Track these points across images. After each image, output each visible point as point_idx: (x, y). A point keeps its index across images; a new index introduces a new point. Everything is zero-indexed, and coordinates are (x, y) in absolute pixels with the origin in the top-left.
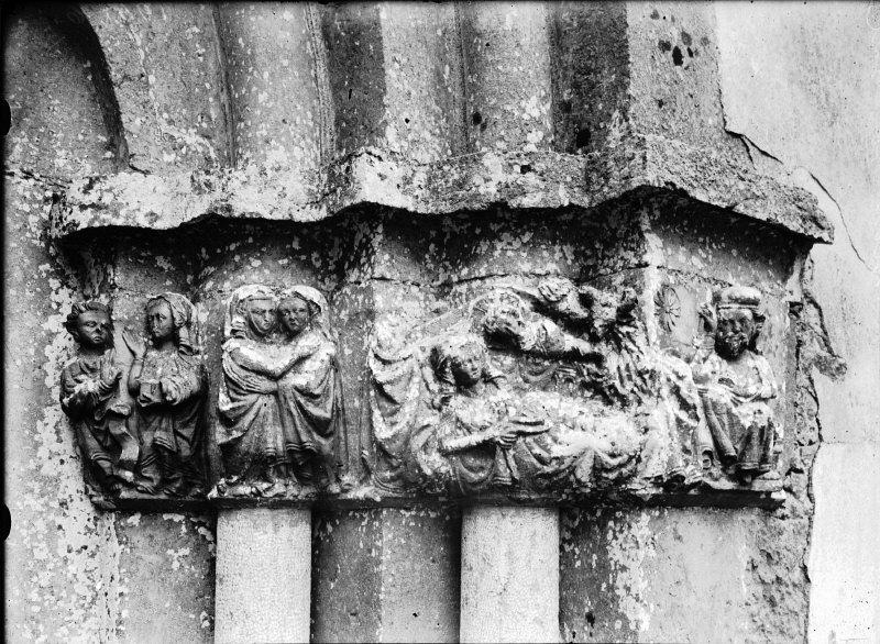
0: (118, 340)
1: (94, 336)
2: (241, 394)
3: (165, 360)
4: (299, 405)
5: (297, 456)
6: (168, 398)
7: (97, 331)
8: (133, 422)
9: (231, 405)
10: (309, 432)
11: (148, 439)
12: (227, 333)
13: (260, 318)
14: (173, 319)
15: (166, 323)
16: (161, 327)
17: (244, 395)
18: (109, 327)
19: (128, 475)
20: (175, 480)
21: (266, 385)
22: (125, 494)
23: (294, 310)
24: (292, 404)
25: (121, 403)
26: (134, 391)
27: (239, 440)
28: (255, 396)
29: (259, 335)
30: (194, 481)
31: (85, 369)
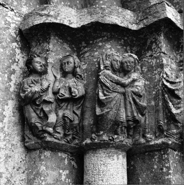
0: (49, 70)
1: (39, 68)
2: (109, 92)
3: (71, 82)
4: (134, 100)
5: (131, 123)
6: (73, 94)
7: (41, 66)
8: (53, 106)
9: (104, 98)
10: (137, 112)
11: (61, 113)
12: (102, 68)
13: (115, 63)
14: (75, 63)
15: (72, 65)
16: (68, 68)
17: (111, 93)
18: (46, 65)
19: (51, 130)
20: (69, 135)
21: (122, 90)
22: (49, 139)
23: (129, 62)
24: (131, 98)
25: (49, 97)
26: (55, 93)
27: (108, 113)
28: (117, 94)
29: (114, 71)
30: (76, 137)
31: (34, 82)
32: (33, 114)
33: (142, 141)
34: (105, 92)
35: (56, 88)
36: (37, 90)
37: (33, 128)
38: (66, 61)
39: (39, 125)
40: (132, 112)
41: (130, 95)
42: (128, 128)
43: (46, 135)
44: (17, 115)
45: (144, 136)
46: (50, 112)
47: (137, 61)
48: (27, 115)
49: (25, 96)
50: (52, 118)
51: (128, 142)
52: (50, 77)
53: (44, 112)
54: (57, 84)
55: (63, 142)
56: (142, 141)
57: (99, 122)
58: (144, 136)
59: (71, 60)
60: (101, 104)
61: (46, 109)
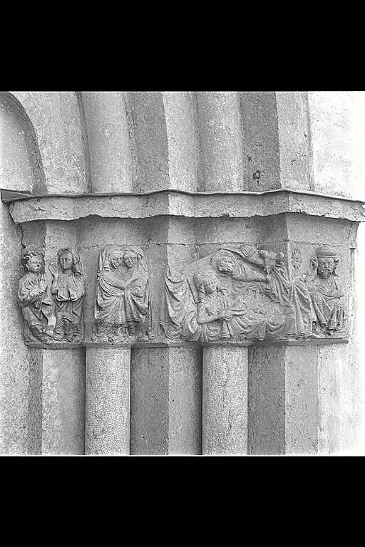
3: (71, 279)
4: (133, 301)
7: (38, 266)
12: (101, 269)
16: (67, 265)
19: (51, 332)
25: (48, 299)
32: (33, 317)
33: (146, 338)
34: (104, 297)
35: (54, 291)
36: (35, 293)
37: (33, 330)
38: (64, 257)
39: (39, 328)
40: (131, 313)
41: (129, 297)
42: (129, 328)
43: (47, 338)
44: (16, 314)
45: (147, 334)
46: (49, 314)
47: (139, 256)
48: (26, 317)
49: (24, 299)
50: (52, 321)
51: (131, 339)
52: (47, 276)
53: (44, 315)
54: (55, 284)
55: (65, 342)
56: (146, 338)
57: (98, 324)
58: (147, 334)
59: (69, 256)
60: (100, 308)
61: (45, 312)
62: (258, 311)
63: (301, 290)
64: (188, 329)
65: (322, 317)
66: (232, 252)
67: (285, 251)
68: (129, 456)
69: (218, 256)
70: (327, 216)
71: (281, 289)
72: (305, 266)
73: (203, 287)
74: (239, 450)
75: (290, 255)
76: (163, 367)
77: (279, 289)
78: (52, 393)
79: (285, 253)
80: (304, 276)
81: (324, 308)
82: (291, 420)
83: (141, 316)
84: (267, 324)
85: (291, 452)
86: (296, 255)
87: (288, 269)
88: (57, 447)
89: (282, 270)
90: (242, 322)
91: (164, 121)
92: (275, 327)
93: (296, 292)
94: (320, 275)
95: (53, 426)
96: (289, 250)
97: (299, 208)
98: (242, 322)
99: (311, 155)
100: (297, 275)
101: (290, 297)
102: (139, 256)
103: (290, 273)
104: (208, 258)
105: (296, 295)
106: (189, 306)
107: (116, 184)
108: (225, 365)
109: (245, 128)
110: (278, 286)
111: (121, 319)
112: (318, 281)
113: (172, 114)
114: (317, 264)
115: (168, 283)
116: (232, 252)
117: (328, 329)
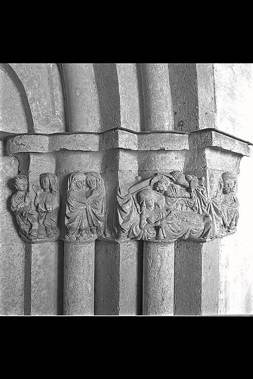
46: (33, 221)
47: (98, 179)
62: (185, 220)
63: (216, 204)
64: (133, 233)
65: (226, 221)
66: (167, 176)
67: (205, 176)
68: (93, 315)
69: (155, 180)
70: (232, 151)
71: (201, 203)
72: (216, 186)
73: (144, 203)
74: (168, 312)
75: (208, 178)
76: (116, 257)
77: (199, 203)
78: (39, 273)
79: (206, 178)
80: (215, 193)
81: (228, 215)
82: (205, 292)
83: (99, 222)
84: (191, 230)
85: (204, 314)
86: (212, 179)
87: (207, 190)
88: (44, 308)
89: (203, 189)
90: (173, 228)
91: (117, 84)
92: (196, 231)
93: (212, 206)
94: (225, 192)
95: (41, 295)
96: (208, 175)
97: (219, 143)
98: (173, 228)
99: (216, 111)
100: (212, 190)
101: (207, 210)
102: (98, 179)
103: (208, 192)
104: (148, 181)
105: (212, 208)
106: (135, 216)
107: (84, 128)
108: (159, 256)
109: (173, 94)
110: (199, 201)
111: (85, 224)
112: (223, 196)
113: (123, 80)
114: (223, 184)
115: (119, 199)
116: (167, 176)
117: (229, 229)
